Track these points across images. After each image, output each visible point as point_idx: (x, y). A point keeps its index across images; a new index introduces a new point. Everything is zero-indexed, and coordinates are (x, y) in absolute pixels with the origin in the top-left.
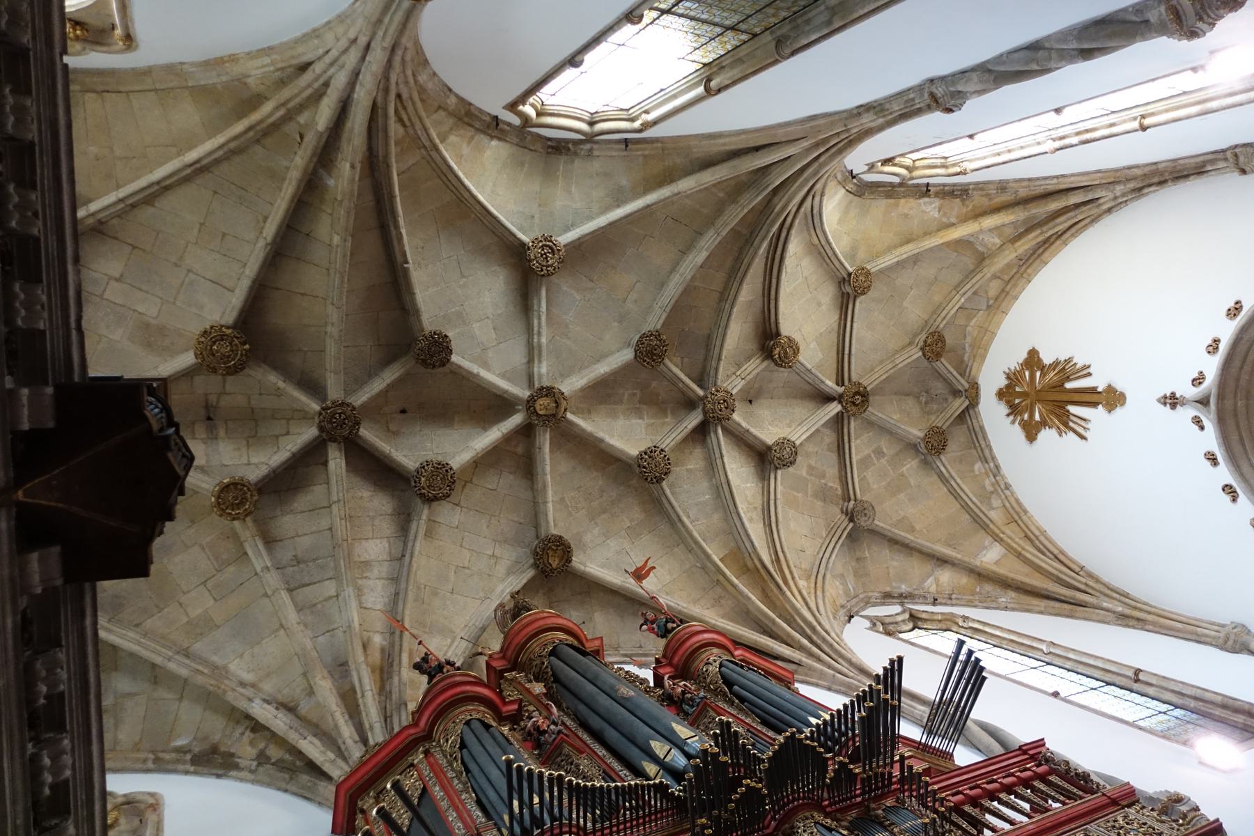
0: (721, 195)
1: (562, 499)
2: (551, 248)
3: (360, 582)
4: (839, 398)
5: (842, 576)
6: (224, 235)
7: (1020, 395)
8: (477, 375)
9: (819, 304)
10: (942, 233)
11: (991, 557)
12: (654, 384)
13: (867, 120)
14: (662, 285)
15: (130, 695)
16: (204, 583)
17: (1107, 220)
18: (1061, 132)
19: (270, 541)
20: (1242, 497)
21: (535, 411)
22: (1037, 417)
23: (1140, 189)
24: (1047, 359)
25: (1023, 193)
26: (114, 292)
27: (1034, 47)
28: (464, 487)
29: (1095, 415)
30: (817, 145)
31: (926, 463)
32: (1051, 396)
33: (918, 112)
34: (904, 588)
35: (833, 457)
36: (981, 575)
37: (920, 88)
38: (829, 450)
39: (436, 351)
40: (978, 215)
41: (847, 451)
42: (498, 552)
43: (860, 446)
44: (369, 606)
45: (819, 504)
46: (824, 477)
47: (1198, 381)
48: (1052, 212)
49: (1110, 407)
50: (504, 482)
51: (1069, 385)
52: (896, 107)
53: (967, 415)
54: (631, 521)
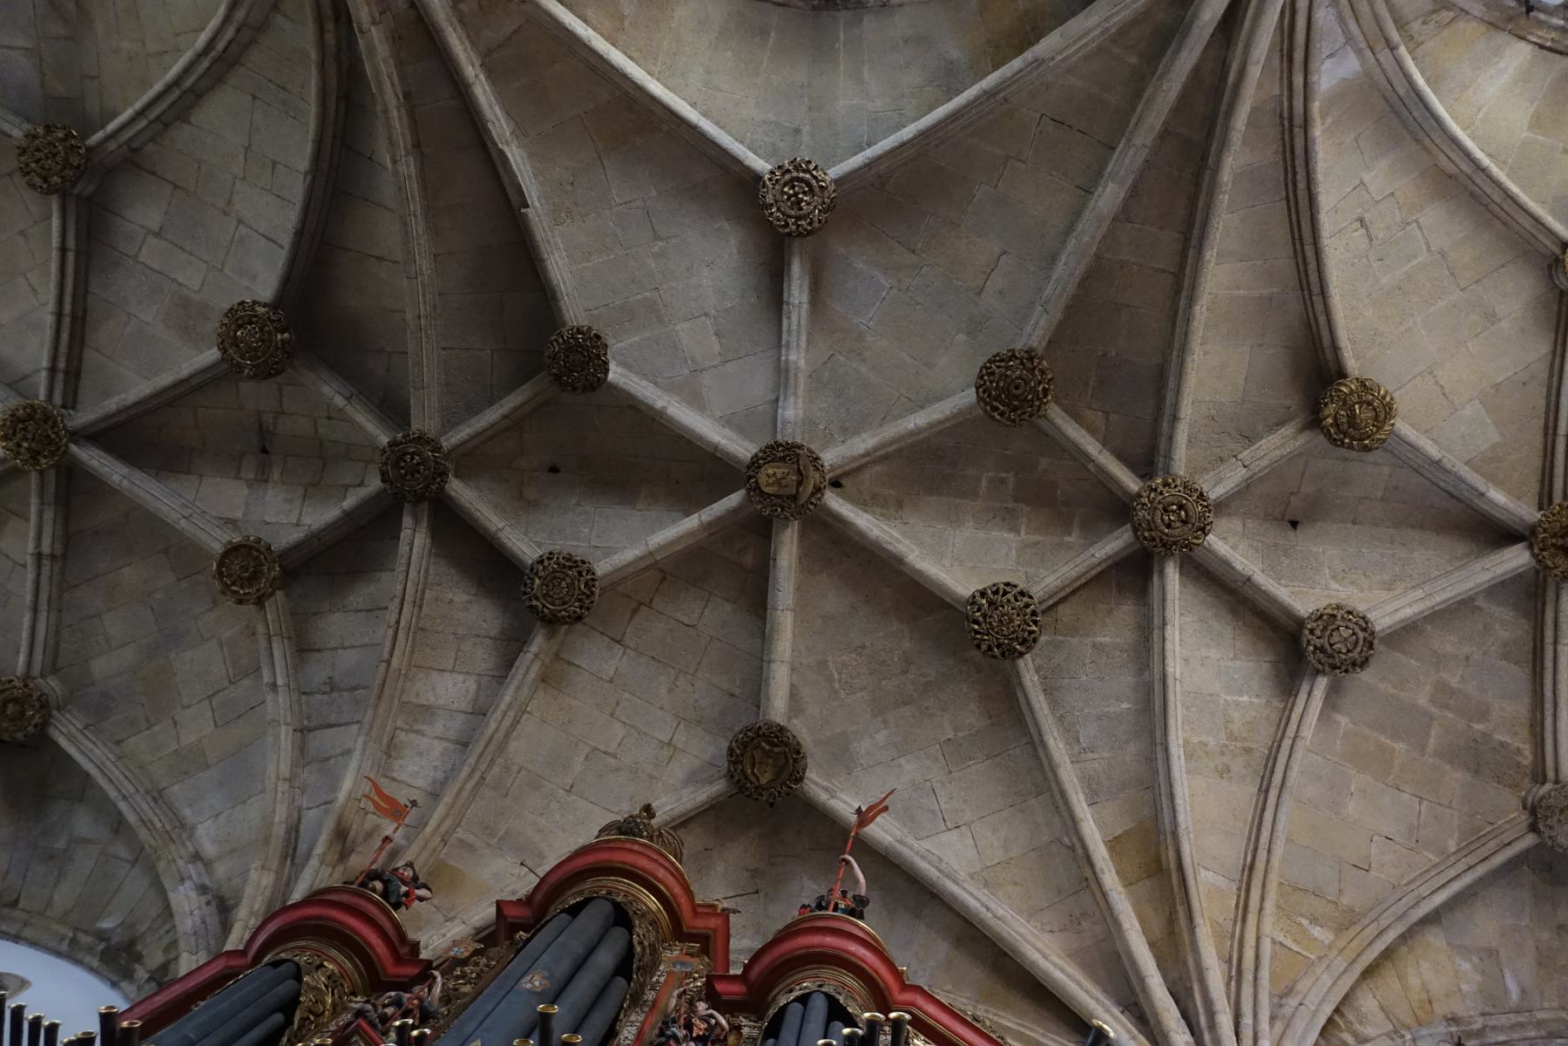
0: (1133, 60)
1: (822, 664)
2: (808, 184)
3: (402, 736)
5: (1492, 953)
6: (274, 164)
8: (662, 413)
9: (1491, 317)
12: (1044, 463)
14: (1053, 259)
15: (85, 841)
16: (210, 698)
19: (303, 649)
21: (758, 487)
26: (151, 253)
28: (635, 611)
35: (1519, 675)
38: (1505, 656)
39: (582, 359)
41: (1549, 664)
42: (680, 739)
44: (403, 777)
45: (1455, 778)
46: (1483, 715)
50: (711, 615)
54: (956, 729)
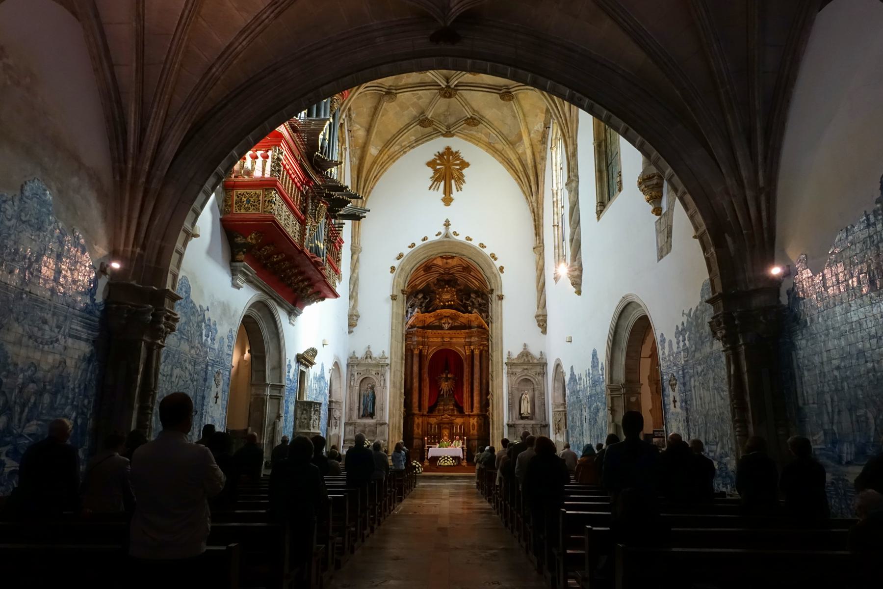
4: (448, 87)
7: (448, 158)
10: (526, 131)
11: (373, 151)
13: (570, 148)
17: (524, 197)
18: (559, 194)
20: (410, 250)
22: (438, 167)
23: (534, 212)
24: (464, 171)
25: (539, 167)
27: (578, 223)
29: (440, 193)
30: (566, 120)
31: (415, 117)
32: (448, 172)
33: (569, 172)
34: (353, 116)
35: (418, 81)
36: (364, 148)
37: (577, 176)
40: (532, 145)
43: (425, 95)
47: (455, 233)
48: (530, 178)
49: (444, 200)
51: (453, 181)
52: (572, 163)
53: (437, 133)
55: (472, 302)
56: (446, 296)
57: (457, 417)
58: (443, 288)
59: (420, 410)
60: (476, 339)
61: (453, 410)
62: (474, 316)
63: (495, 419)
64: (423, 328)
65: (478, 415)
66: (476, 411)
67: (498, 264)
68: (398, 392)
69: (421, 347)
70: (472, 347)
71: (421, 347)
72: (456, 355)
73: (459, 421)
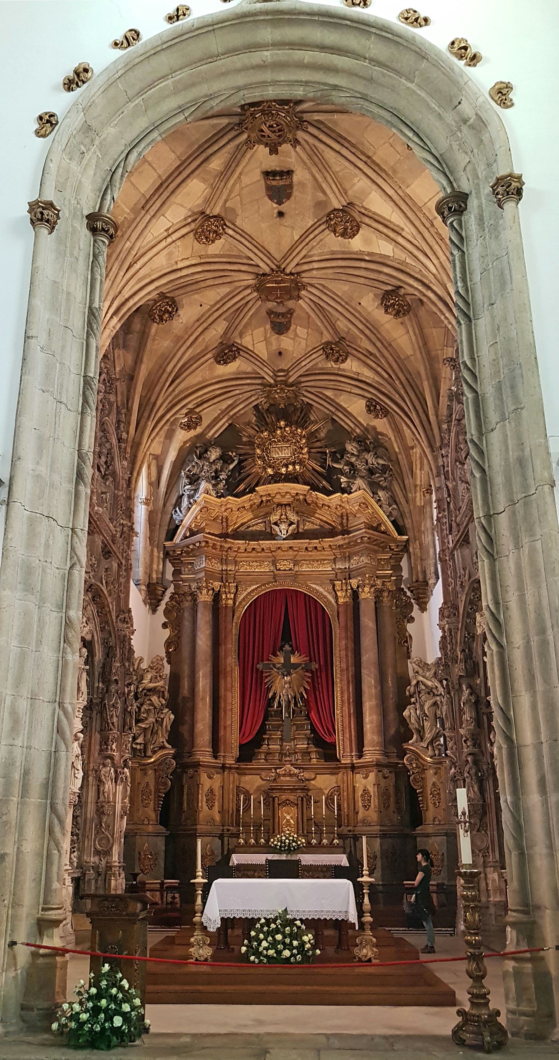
55: (351, 465)
56: (282, 453)
57: (318, 771)
58: (272, 432)
59: (216, 757)
60: (365, 560)
61: (306, 753)
62: (357, 501)
63: (527, 736)
64: (224, 536)
65: (378, 765)
66: (372, 753)
67: (483, 78)
68: (52, 621)
69: (217, 584)
70: (354, 582)
71: (217, 584)
72: (311, 604)
73: (324, 782)
